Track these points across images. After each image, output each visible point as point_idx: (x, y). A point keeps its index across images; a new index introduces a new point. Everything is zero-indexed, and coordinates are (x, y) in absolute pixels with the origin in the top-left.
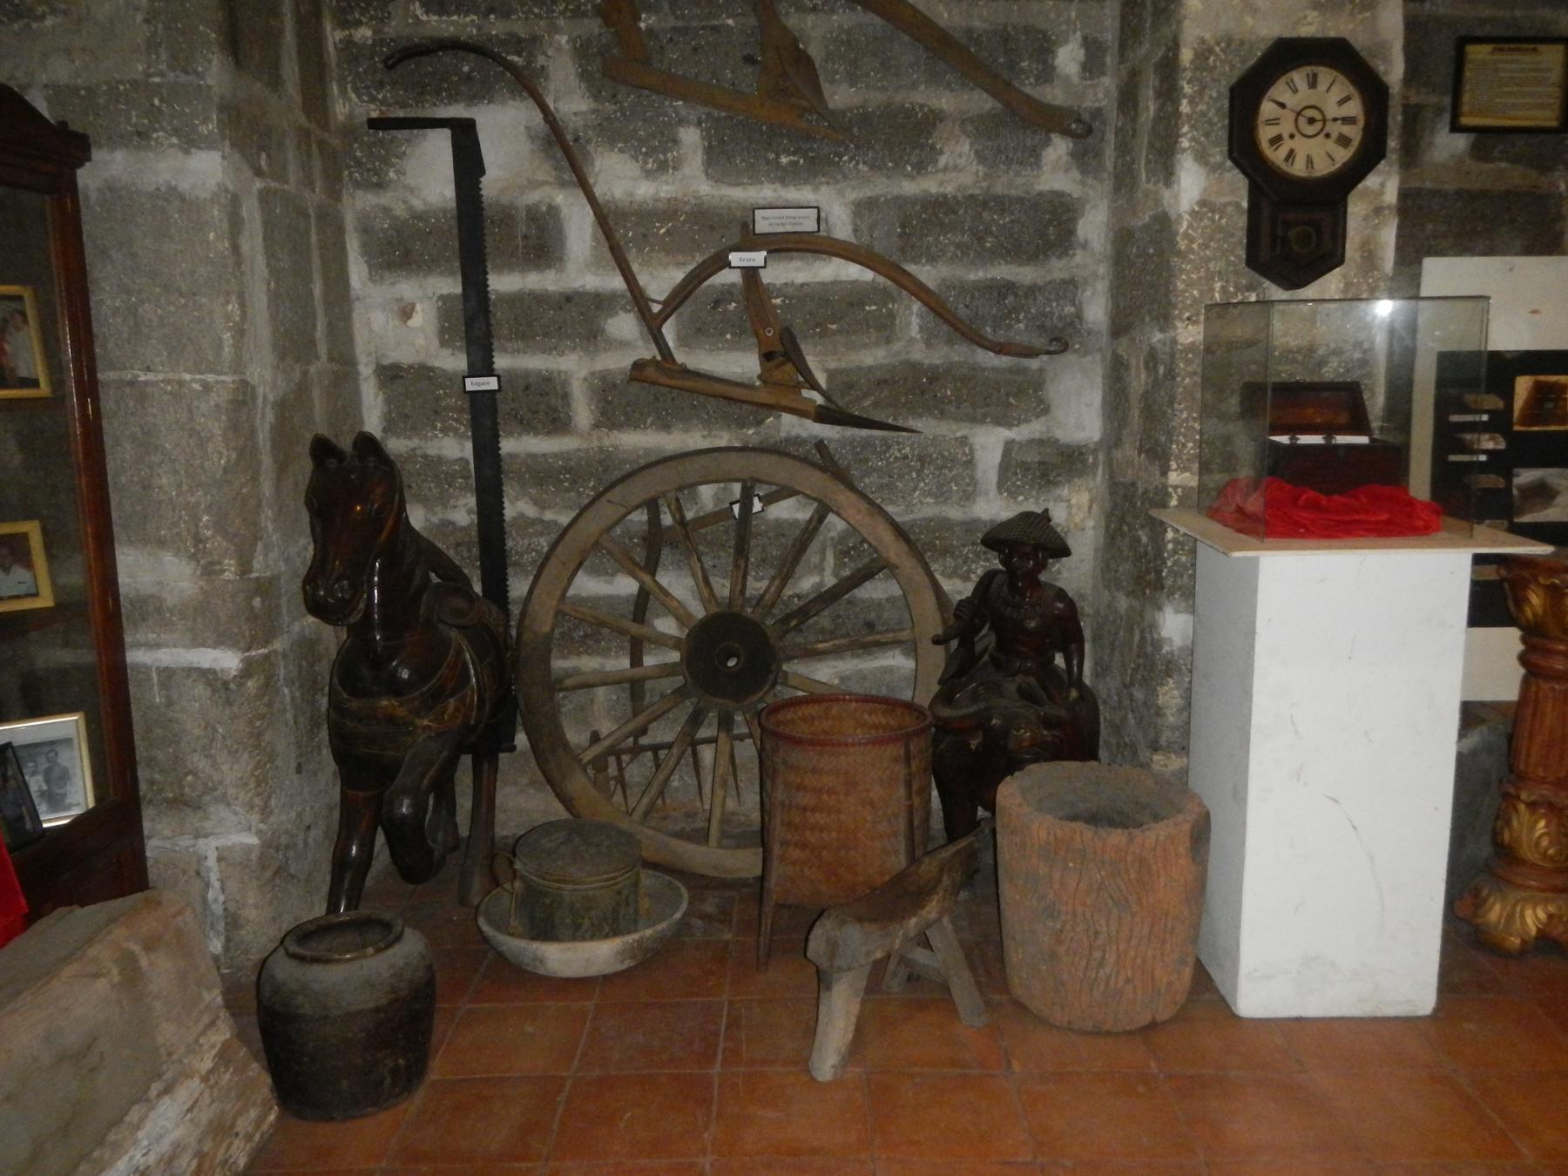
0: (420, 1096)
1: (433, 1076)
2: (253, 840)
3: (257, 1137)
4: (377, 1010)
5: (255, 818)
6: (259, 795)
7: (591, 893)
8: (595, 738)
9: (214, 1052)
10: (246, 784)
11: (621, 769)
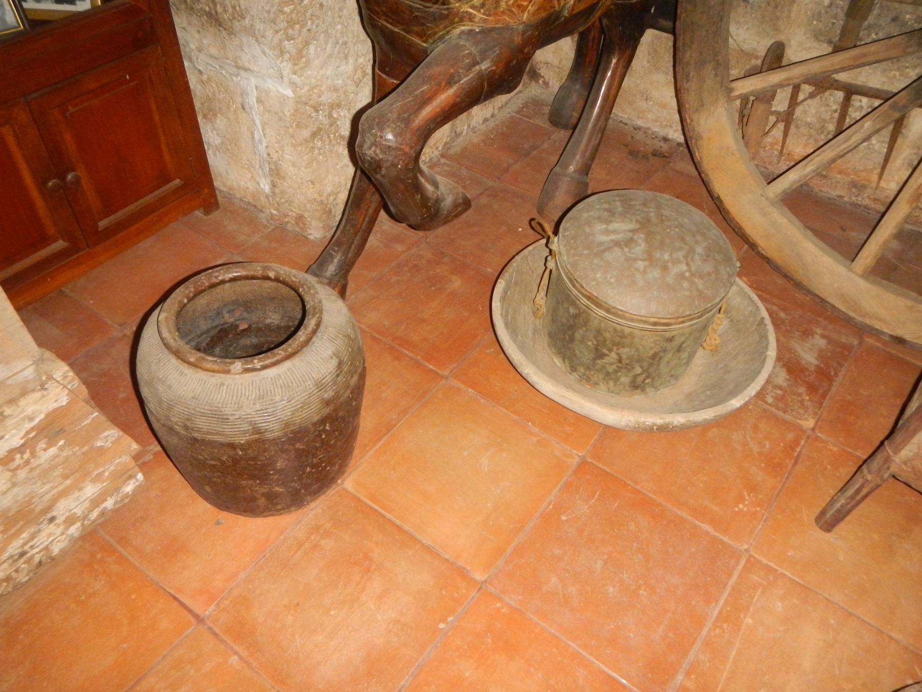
0: (316, 510)
1: (349, 483)
2: (289, 92)
3: (94, 514)
4: (232, 446)
5: (286, 67)
6: (289, 38)
7: (627, 331)
8: (775, 58)
9: (28, 425)
10: (274, 21)
11: (793, 102)
